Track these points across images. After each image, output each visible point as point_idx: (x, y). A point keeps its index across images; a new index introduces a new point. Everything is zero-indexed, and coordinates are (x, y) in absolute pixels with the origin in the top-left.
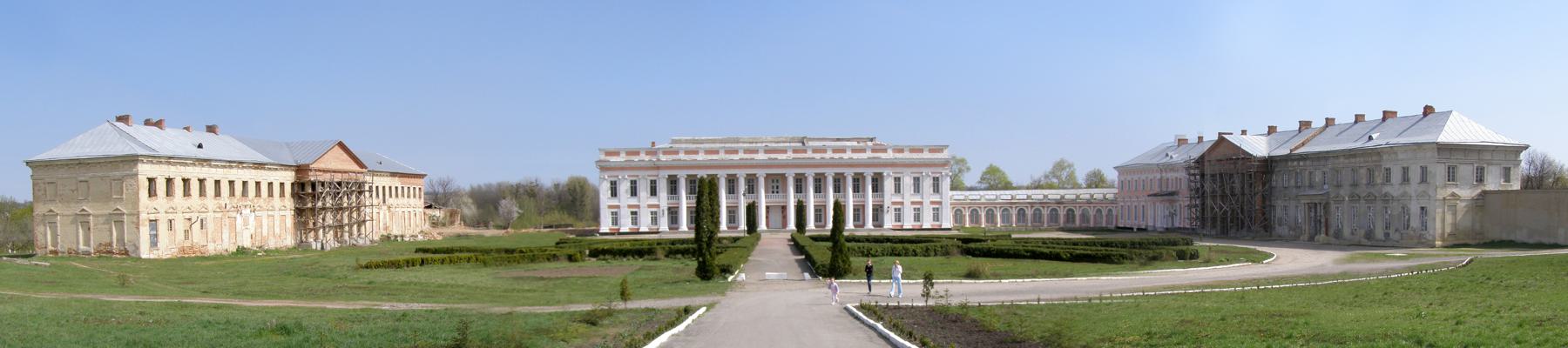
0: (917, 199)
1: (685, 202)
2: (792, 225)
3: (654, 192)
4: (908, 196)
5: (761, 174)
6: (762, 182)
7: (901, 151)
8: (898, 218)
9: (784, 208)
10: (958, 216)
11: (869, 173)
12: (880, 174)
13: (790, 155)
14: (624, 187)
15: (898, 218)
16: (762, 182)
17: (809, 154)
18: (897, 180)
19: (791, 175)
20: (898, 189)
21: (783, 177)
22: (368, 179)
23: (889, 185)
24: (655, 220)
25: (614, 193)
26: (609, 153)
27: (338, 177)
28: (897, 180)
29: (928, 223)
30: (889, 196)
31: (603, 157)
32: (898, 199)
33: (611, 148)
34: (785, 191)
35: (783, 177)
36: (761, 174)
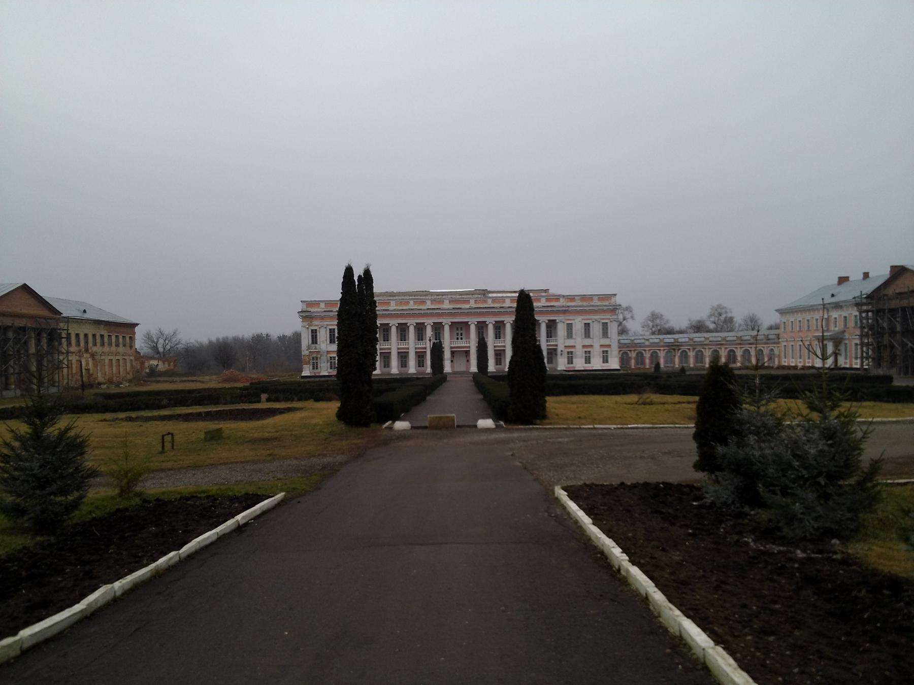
0: (587, 342)
2: (474, 368)
4: (579, 341)
5: (446, 321)
6: (447, 328)
8: (570, 361)
9: (467, 353)
10: (624, 359)
12: (555, 320)
13: (472, 304)
15: (570, 361)
16: (447, 328)
17: (490, 304)
18: (570, 327)
19: (473, 321)
20: (570, 335)
21: (467, 325)
22: (62, 325)
23: (561, 330)
25: (314, 340)
27: (20, 323)
28: (570, 327)
29: (597, 364)
32: (570, 342)
34: (468, 337)
35: (467, 325)
36: (446, 321)
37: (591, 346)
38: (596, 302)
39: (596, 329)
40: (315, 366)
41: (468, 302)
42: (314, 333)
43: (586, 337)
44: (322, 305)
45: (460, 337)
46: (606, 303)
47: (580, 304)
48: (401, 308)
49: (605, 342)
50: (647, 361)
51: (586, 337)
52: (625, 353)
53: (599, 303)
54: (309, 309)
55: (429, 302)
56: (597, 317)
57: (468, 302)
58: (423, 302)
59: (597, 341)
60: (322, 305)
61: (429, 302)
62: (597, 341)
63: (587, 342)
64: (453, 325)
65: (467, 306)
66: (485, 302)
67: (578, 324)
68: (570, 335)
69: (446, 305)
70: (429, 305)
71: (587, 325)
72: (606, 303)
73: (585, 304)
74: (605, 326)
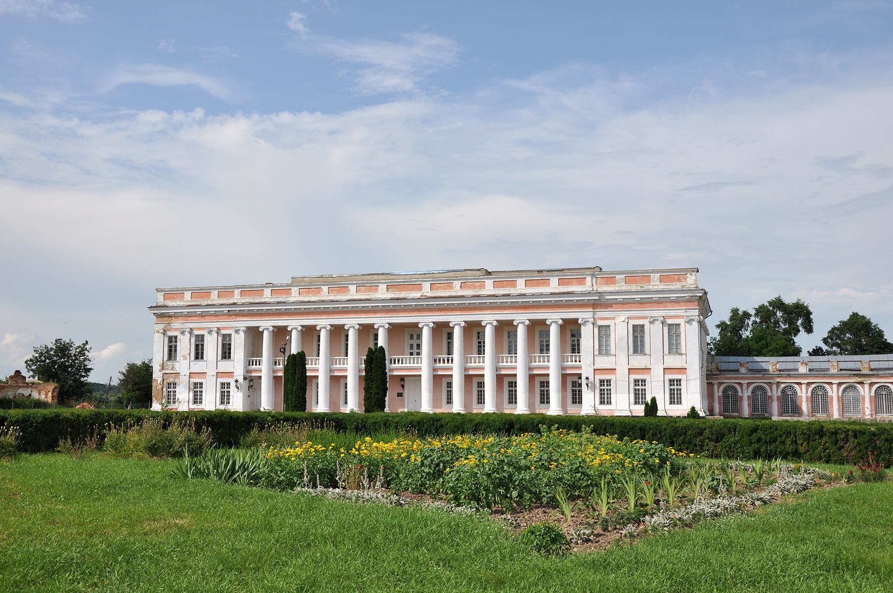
0: (638, 361)
1: (267, 368)
3: (226, 353)
4: (620, 360)
5: (381, 322)
7: (610, 279)
8: (605, 398)
11: (554, 318)
13: (426, 290)
14: (185, 345)
15: (605, 398)
18: (604, 332)
19: (426, 321)
20: (603, 349)
24: (225, 397)
26: (170, 294)
30: (586, 364)
31: (160, 299)
32: (604, 362)
33: (171, 284)
37: (647, 370)
38: (655, 284)
39: (655, 336)
40: (171, 397)
41: (419, 287)
42: (173, 341)
43: (635, 351)
44: (188, 295)
45: (415, 351)
46: (677, 286)
47: (624, 287)
48: (307, 299)
49: (674, 361)
50: (805, 407)
51: (635, 351)
52: (820, 387)
53: (661, 287)
54: (170, 303)
55: (353, 288)
56: (659, 313)
57: (419, 287)
58: (344, 289)
59: (656, 361)
60: (188, 295)
61: (353, 288)
62: (656, 361)
63: (638, 361)
64: (395, 330)
65: (417, 295)
66: (450, 287)
67: (620, 324)
68: (603, 349)
69: (382, 293)
70: (353, 293)
71: (638, 331)
72: (677, 286)
73: (634, 288)
74: (673, 332)
